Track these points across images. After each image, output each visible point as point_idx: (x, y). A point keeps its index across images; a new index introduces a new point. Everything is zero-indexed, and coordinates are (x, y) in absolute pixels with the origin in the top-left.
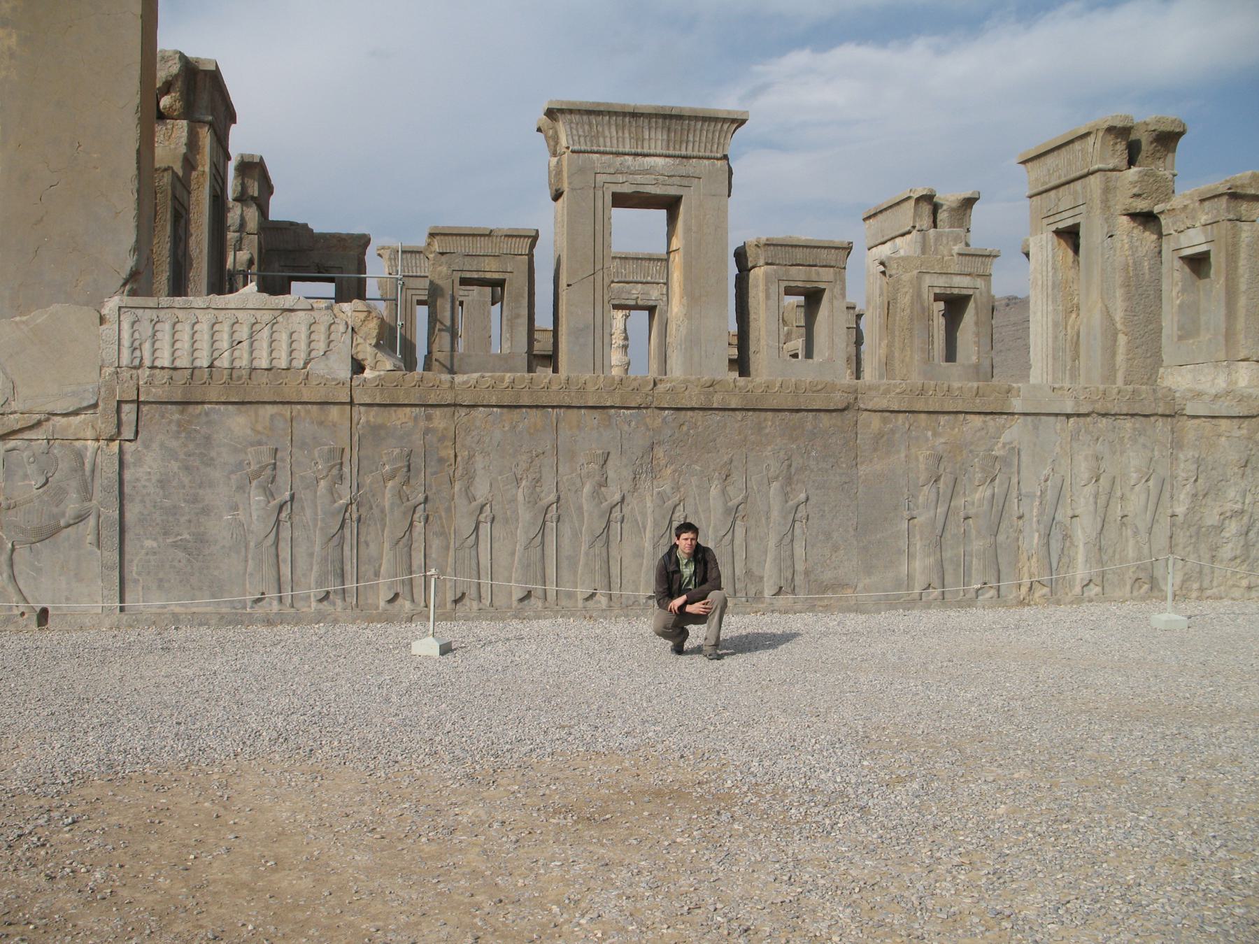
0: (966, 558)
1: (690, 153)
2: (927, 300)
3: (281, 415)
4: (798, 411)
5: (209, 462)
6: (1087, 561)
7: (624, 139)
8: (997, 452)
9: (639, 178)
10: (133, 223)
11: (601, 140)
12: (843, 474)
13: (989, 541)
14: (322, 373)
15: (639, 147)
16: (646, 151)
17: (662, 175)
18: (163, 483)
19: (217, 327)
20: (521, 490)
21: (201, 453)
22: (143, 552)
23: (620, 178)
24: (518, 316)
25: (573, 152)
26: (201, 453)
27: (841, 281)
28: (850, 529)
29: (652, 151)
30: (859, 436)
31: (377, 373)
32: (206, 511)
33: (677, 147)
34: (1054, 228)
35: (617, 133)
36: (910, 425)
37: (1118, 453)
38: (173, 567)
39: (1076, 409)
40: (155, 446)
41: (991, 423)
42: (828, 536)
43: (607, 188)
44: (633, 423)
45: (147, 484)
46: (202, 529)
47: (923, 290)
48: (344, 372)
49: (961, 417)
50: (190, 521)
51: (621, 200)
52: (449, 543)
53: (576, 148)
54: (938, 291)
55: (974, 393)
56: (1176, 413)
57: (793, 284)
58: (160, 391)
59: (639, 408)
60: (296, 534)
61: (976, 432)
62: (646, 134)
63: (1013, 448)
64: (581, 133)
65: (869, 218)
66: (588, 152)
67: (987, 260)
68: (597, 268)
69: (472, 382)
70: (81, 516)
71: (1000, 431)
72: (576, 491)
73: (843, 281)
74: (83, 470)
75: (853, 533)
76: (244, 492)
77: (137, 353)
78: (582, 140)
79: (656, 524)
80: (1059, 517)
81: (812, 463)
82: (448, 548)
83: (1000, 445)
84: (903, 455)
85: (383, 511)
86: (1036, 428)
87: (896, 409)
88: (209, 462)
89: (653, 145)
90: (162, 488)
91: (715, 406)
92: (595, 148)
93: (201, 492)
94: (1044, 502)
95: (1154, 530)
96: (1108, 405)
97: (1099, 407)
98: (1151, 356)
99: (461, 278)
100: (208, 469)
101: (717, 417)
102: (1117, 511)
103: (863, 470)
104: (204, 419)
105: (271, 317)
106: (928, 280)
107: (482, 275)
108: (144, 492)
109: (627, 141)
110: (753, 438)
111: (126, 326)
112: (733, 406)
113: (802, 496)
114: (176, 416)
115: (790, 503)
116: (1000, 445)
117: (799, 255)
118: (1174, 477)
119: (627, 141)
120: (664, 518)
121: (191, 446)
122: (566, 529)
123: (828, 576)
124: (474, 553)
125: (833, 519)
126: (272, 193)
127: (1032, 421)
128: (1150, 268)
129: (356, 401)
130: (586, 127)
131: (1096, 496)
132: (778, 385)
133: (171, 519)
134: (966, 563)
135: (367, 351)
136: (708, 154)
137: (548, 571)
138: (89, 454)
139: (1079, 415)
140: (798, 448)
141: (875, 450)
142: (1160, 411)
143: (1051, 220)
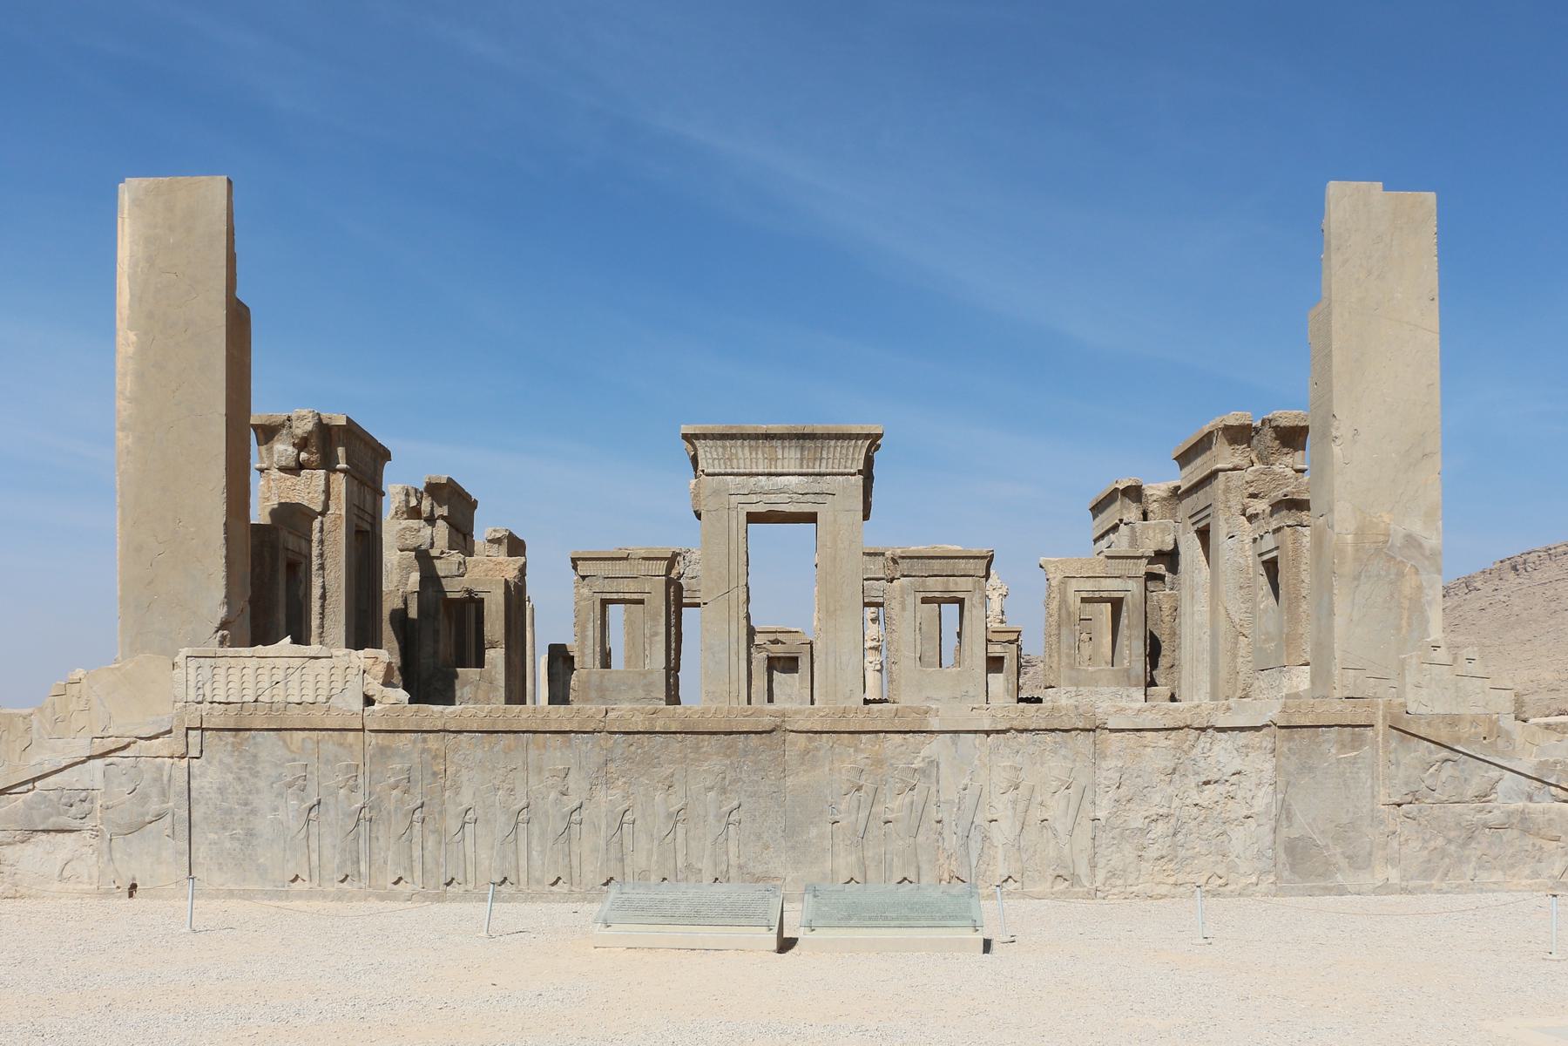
0: (887, 856)
1: (823, 470)
2: (1073, 606)
3: (311, 739)
4: (731, 733)
5: (256, 775)
6: (1005, 859)
7: (757, 459)
8: (917, 764)
9: (773, 498)
10: (223, 582)
11: (735, 460)
12: (772, 785)
13: (907, 841)
14: (340, 706)
15: (773, 466)
16: (779, 470)
18: (221, 790)
19: (259, 671)
20: (497, 797)
21: (250, 768)
22: (207, 842)
23: (754, 498)
24: (656, 634)
25: (708, 475)
26: (250, 768)
27: (980, 590)
28: (779, 831)
29: (785, 470)
31: (383, 706)
32: (253, 812)
33: (811, 464)
34: (1195, 527)
35: (751, 454)
36: (834, 743)
37: (1038, 765)
38: (230, 854)
39: (994, 726)
40: (215, 762)
41: (912, 740)
42: (759, 837)
43: (742, 508)
44: (589, 745)
45: (209, 790)
46: (251, 827)
47: (1068, 595)
48: (358, 704)
49: (882, 735)
50: (242, 819)
51: (753, 518)
52: (441, 839)
53: (710, 470)
54: (1085, 595)
55: (893, 715)
56: (1097, 727)
58: (217, 720)
59: (593, 732)
60: (322, 830)
61: (896, 748)
63: (932, 761)
65: (869, 554)
67: (1139, 561)
69: (458, 712)
70: (159, 815)
72: (543, 799)
73: (983, 590)
74: (162, 780)
75: (781, 834)
76: (282, 797)
77: (201, 691)
79: (608, 826)
80: (977, 821)
81: (744, 776)
82: (440, 843)
83: (920, 759)
84: (827, 769)
85: (389, 813)
88: (256, 775)
89: (786, 465)
90: (221, 793)
92: (729, 471)
93: (250, 797)
94: (962, 808)
95: (1075, 832)
96: (1027, 722)
97: (1017, 724)
99: (601, 599)
100: (256, 780)
101: (659, 739)
102: (1036, 814)
103: (790, 781)
104: (251, 741)
105: (300, 663)
106: (1074, 585)
107: (621, 596)
108: (208, 796)
109: (760, 461)
110: (692, 756)
111: (192, 671)
112: (674, 730)
113: (735, 803)
114: (231, 740)
115: (724, 809)
116: (920, 759)
117: (937, 566)
119: (760, 461)
120: (615, 820)
121: (243, 762)
122: (535, 829)
123: (759, 870)
124: (461, 847)
126: (476, 508)
127: (951, 737)
129: (366, 728)
130: (720, 450)
131: (1015, 802)
132: (713, 711)
133: (228, 817)
134: (887, 861)
135: (375, 688)
136: (842, 470)
137: (521, 862)
138: (167, 767)
139: (998, 732)
140: (732, 763)
141: (802, 764)
142: (1081, 726)
143: (1194, 520)
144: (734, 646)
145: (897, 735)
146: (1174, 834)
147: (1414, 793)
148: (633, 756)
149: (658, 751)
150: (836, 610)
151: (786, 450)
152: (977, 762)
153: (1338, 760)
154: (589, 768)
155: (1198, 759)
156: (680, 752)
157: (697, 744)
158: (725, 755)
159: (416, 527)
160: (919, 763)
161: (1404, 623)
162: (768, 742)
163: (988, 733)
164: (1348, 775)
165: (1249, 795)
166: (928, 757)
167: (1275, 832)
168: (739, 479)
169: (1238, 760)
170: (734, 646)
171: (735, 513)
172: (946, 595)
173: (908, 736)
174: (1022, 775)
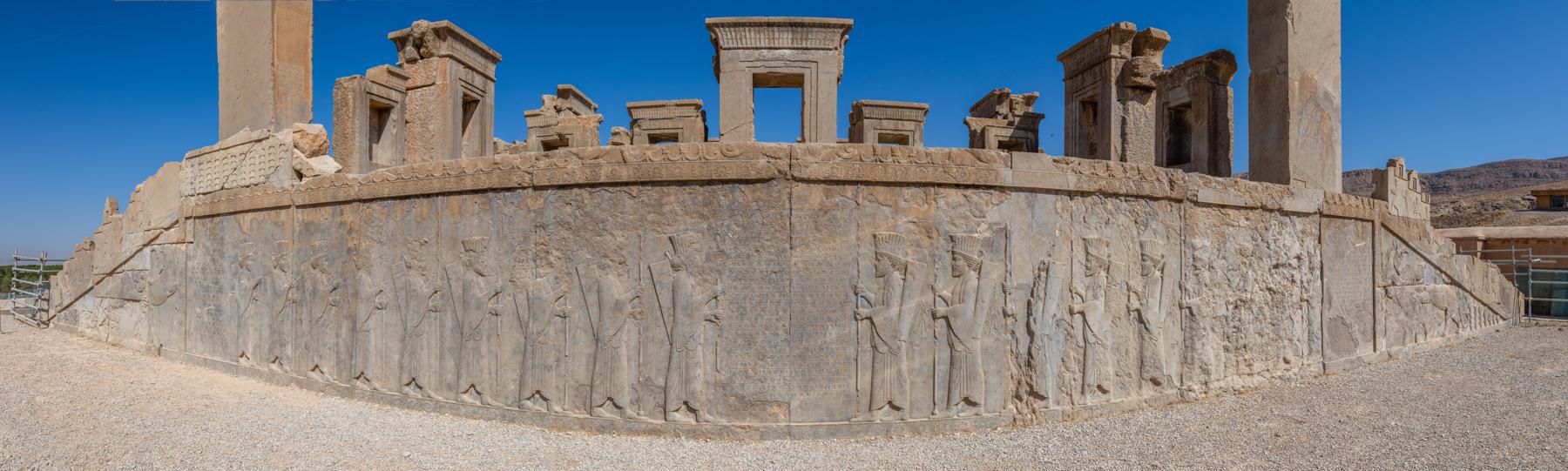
4: (710, 182)
28: (780, 332)
30: (793, 212)
42: (750, 340)
57: (884, 132)
75: (782, 335)
81: (728, 247)
83: (984, 226)
84: (853, 237)
86: (1031, 206)
87: (841, 176)
91: (603, 179)
101: (605, 194)
103: (797, 257)
110: (650, 217)
116: (984, 226)
125: (756, 319)
145: (953, 191)
148: (571, 220)
149: (603, 210)
152: (1057, 233)
154: (513, 238)
156: (636, 213)
157: (661, 198)
158: (702, 216)
160: (984, 231)
162: (764, 196)
163: (1071, 194)
166: (994, 223)
172: (896, 133)
173: (969, 192)
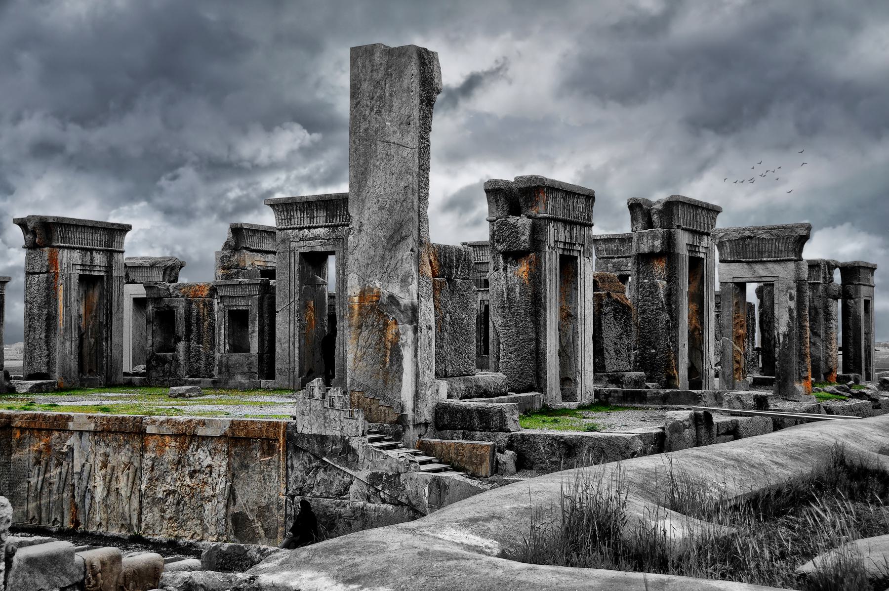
8: (65, 450)
11: (293, 220)
17: (323, 239)
23: (302, 243)
24: (253, 332)
35: (301, 215)
62: (316, 213)
64: (283, 218)
66: (287, 229)
68: (291, 300)
71: (67, 438)
78: (283, 221)
83: (66, 447)
92: (289, 227)
98: (520, 360)
102: (114, 485)
118: (141, 468)
128: (519, 293)
130: (286, 213)
144: (291, 339)
146: (178, 504)
147: (301, 489)
150: (344, 316)
151: (319, 211)
153: (260, 462)
155: (190, 456)
159: (229, 255)
161: (388, 359)
164: (265, 473)
165: (215, 481)
167: (227, 508)
168: (295, 232)
169: (209, 458)
170: (291, 339)
171: (292, 254)
174: (110, 458)
